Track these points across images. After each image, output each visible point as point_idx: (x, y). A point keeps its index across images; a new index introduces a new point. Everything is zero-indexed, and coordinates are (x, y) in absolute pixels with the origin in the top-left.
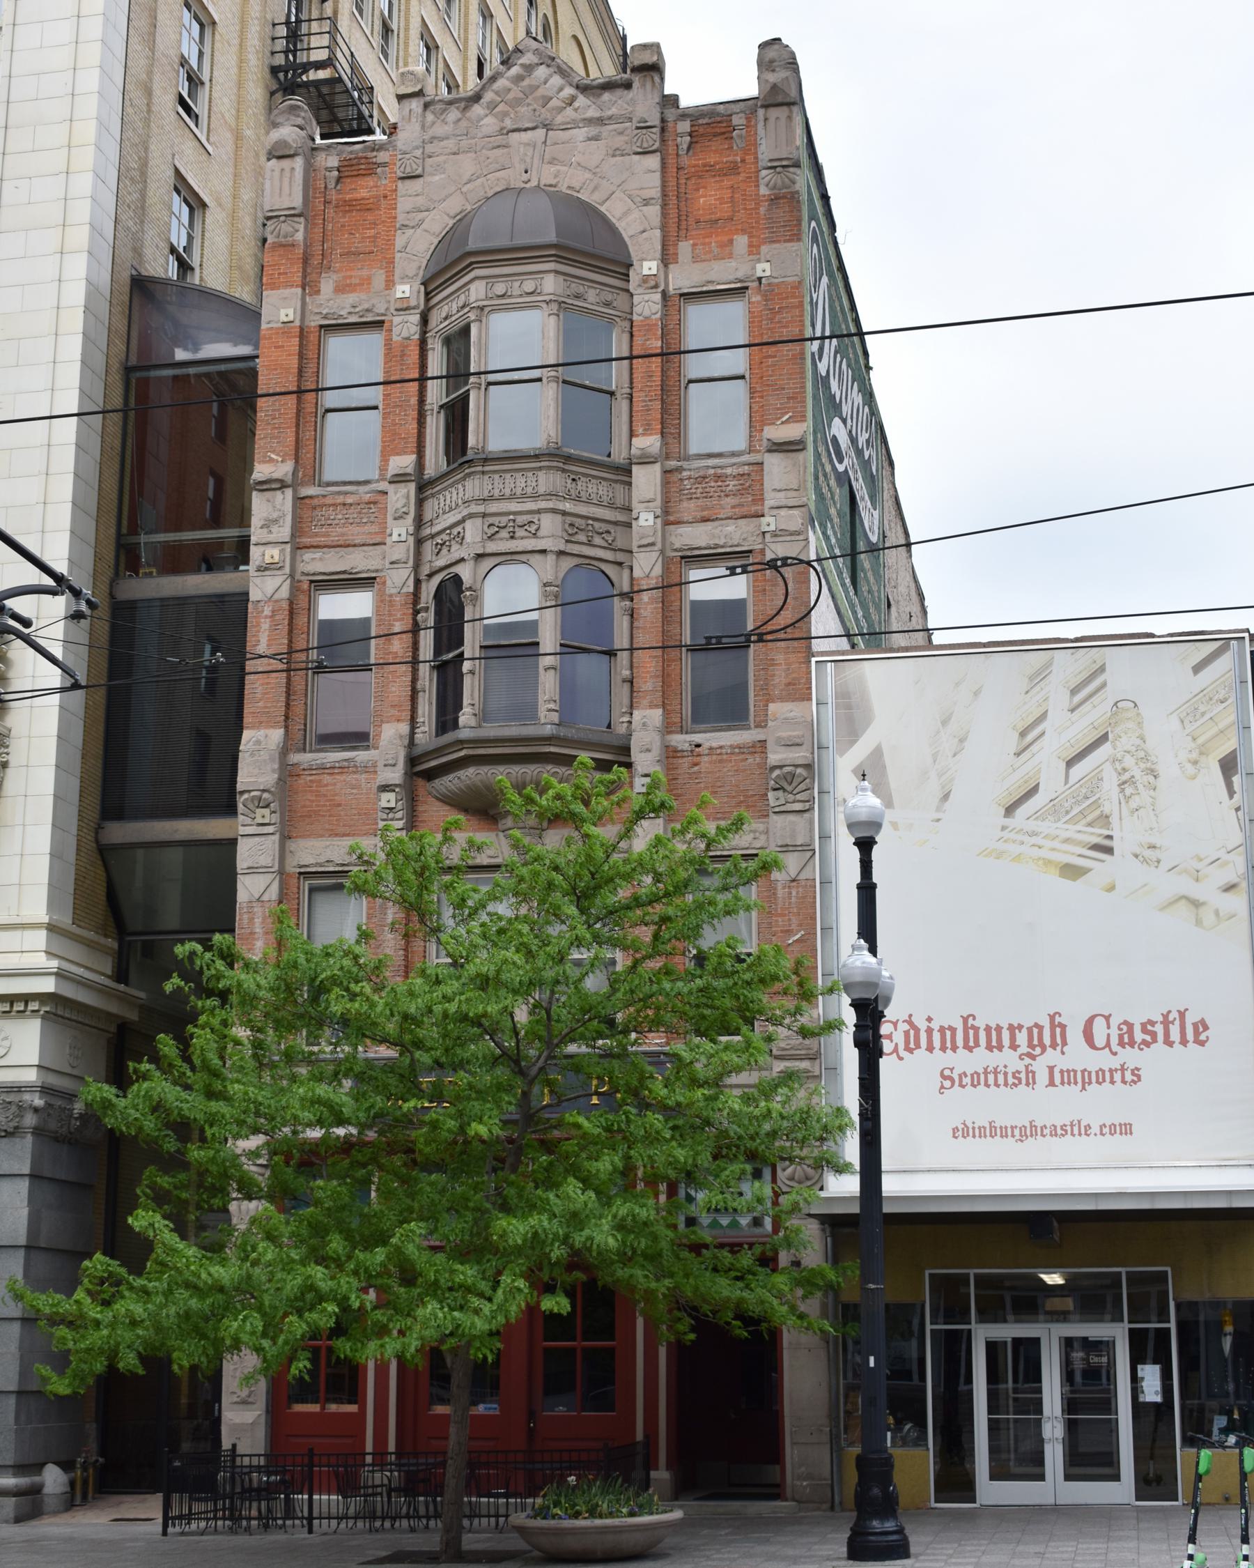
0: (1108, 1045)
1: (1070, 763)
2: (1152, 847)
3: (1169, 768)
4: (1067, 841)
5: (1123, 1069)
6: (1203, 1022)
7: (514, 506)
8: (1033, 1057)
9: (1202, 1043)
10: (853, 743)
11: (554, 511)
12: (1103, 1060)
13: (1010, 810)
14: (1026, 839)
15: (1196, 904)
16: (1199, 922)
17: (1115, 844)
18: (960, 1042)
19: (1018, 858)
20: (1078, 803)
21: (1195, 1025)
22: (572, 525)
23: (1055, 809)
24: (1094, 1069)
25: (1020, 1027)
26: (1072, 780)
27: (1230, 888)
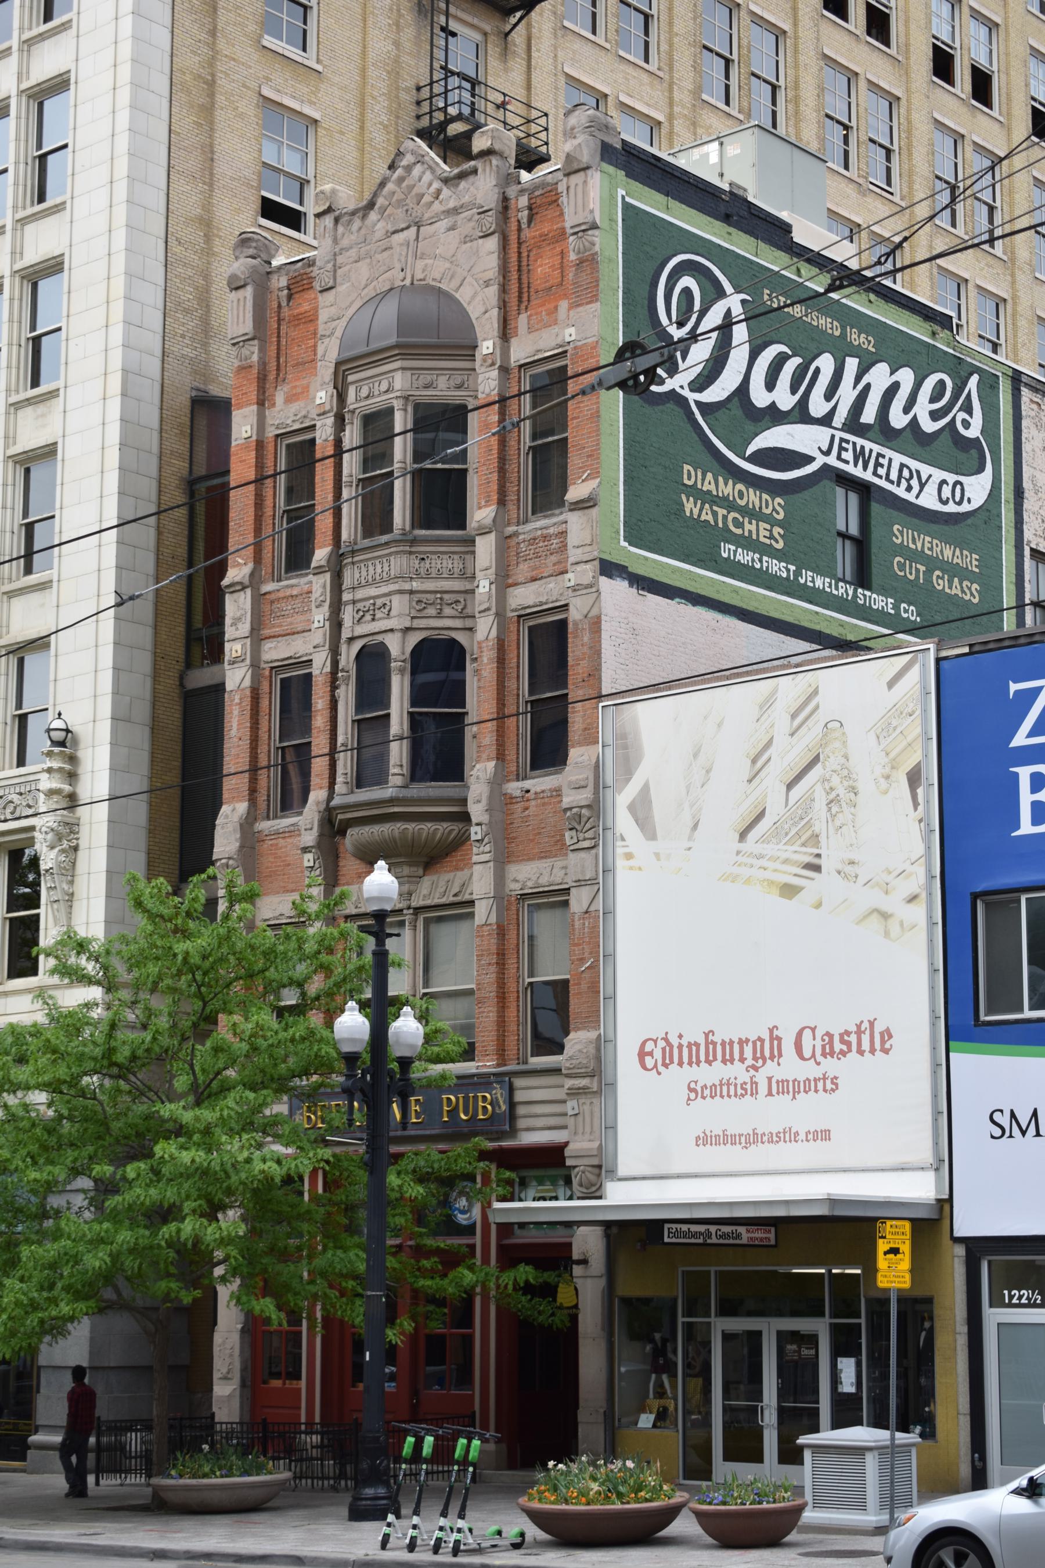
0: (813, 1055)
1: (790, 786)
2: (852, 863)
3: (866, 786)
4: (786, 861)
5: (825, 1078)
6: (888, 1030)
7: (373, 591)
8: (756, 1069)
9: (886, 1051)
10: (628, 780)
11: (401, 592)
12: (808, 1070)
13: (743, 836)
14: (755, 861)
15: (885, 916)
16: (887, 934)
17: (823, 862)
18: (702, 1058)
19: (748, 881)
20: (795, 824)
21: (882, 1034)
22: (419, 602)
23: (777, 832)
24: (801, 1079)
25: (747, 1041)
26: (791, 803)
27: (913, 899)
